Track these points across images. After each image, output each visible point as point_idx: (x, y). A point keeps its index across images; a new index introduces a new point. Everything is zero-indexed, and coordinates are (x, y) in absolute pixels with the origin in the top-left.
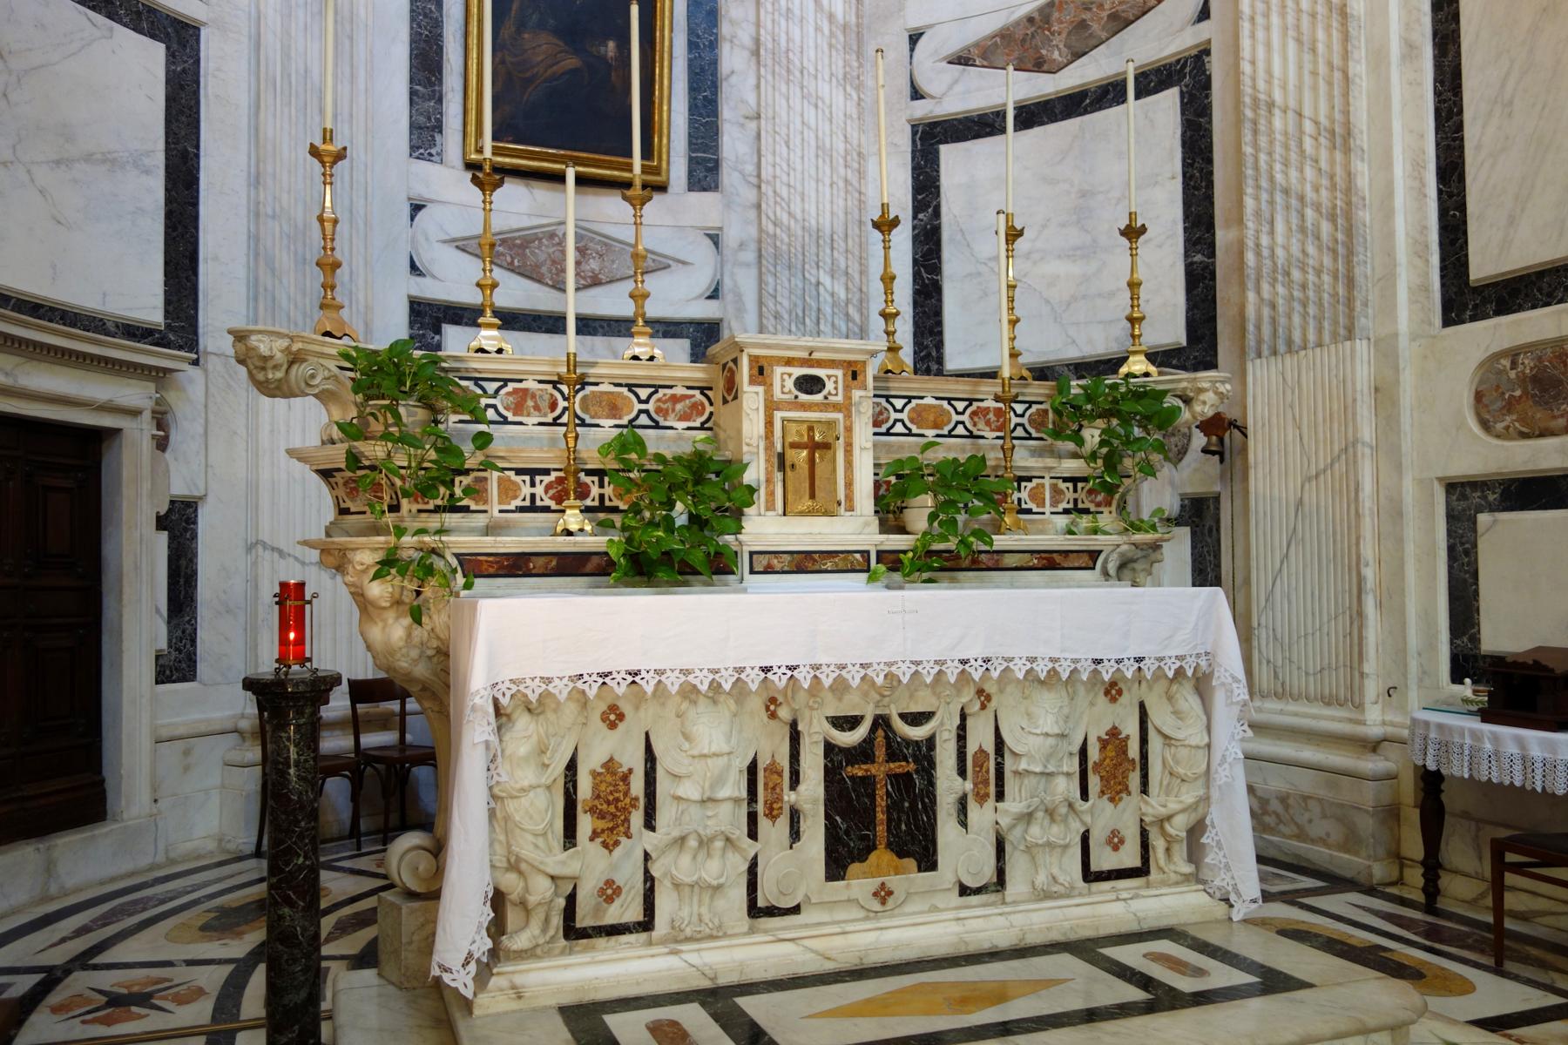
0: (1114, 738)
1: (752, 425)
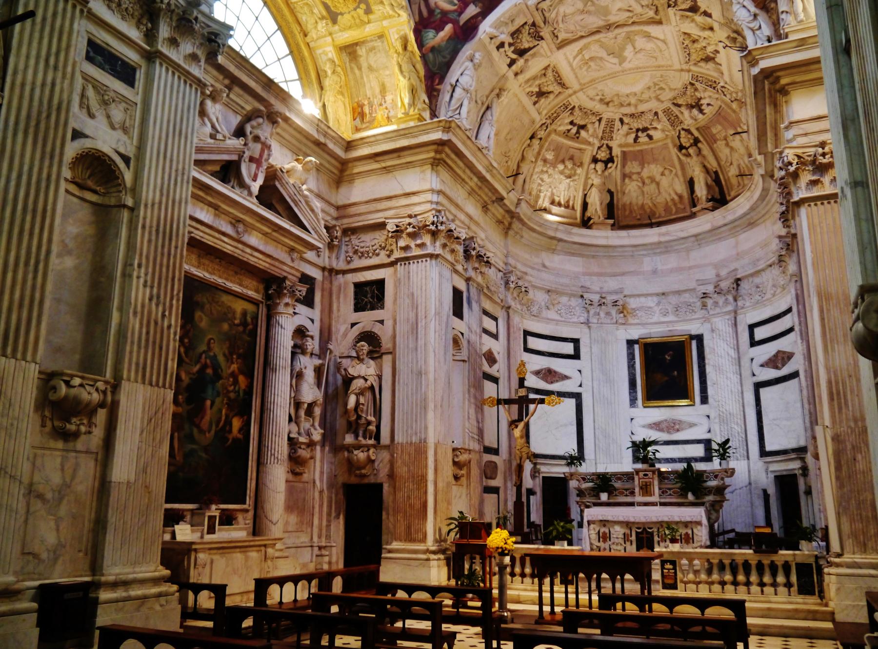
0: (687, 534)
1: (636, 482)
